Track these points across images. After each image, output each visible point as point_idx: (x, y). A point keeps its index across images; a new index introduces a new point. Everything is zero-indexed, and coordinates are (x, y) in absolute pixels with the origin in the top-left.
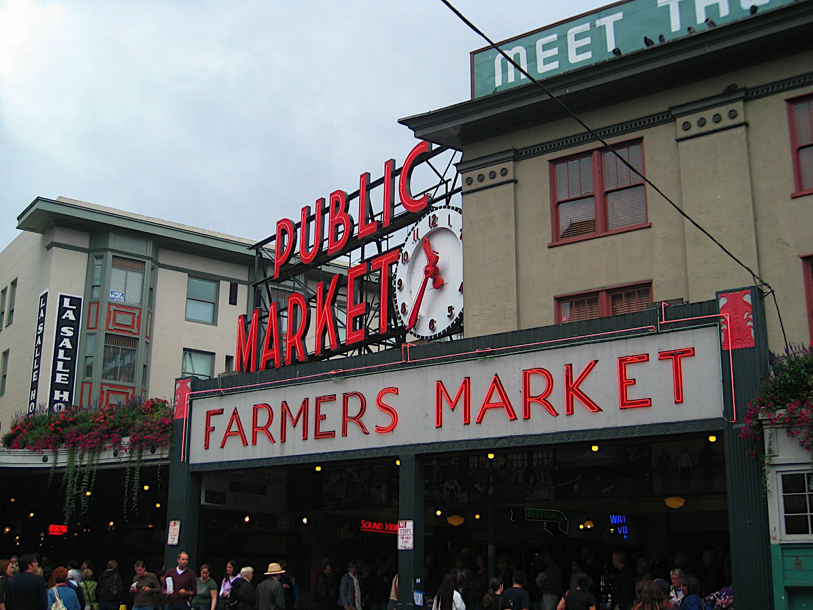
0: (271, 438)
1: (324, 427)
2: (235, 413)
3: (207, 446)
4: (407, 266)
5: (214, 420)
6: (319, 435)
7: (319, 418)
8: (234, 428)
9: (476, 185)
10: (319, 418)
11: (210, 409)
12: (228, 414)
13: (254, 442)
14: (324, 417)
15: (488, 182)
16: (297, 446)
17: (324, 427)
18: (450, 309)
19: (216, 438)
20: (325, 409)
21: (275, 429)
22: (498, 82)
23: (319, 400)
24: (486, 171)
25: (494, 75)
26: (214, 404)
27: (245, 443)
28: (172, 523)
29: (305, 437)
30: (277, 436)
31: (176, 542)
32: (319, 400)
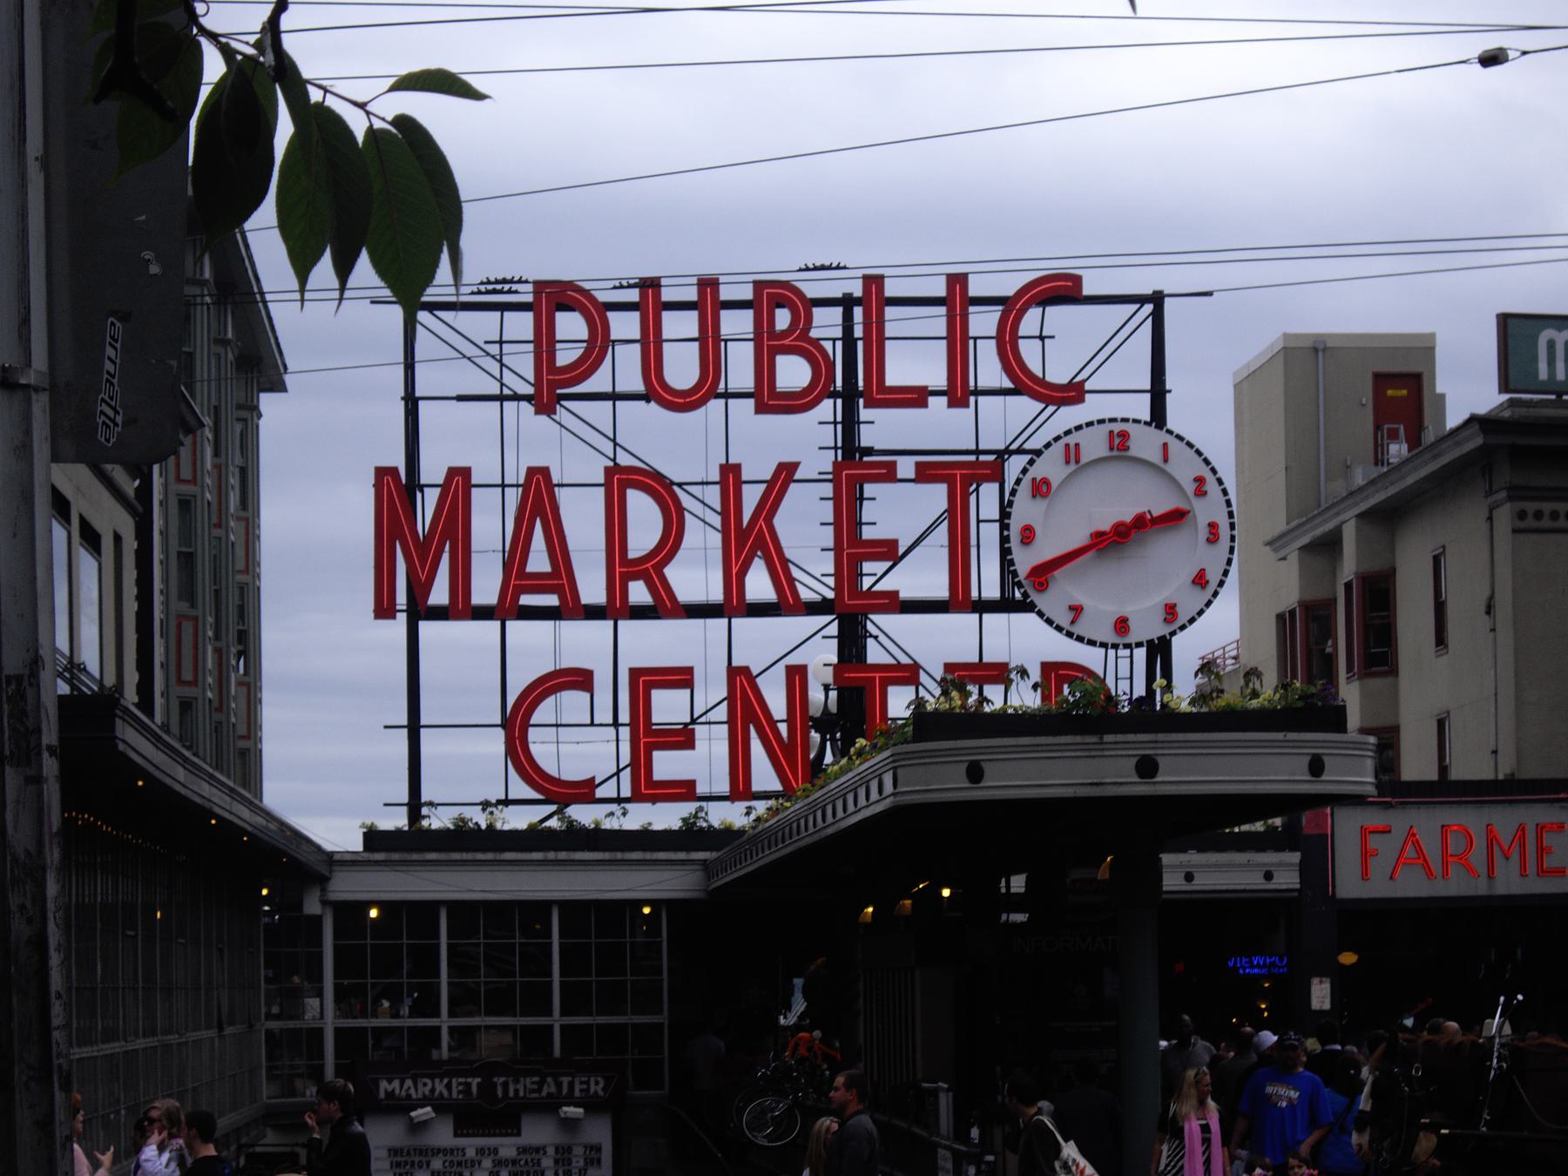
0: (1471, 871)
1: (1548, 862)
2: (1411, 834)
3: (1365, 875)
4: (1041, 504)
5: (1374, 841)
6: (1542, 872)
7: (1542, 851)
8: (1410, 852)
9: (1530, 522)
10: (1542, 851)
11: (1366, 824)
12: (1399, 833)
13: (1445, 873)
14: (1549, 850)
15: (1546, 523)
16: (1510, 881)
17: (1548, 862)
18: (1170, 611)
19: (1380, 866)
20: (1548, 839)
21: (1478, 857)
22: (1543, 374)
23: (1540, 829)
24: (1547, 507)
25: (1535, 359)
26: (1374, 818)
27: (1430, 873)
28: (1315, 981)
29: (1523, 872)
30: (1482, 869)
31: (1327, 1006)
32: (1540, 829)
